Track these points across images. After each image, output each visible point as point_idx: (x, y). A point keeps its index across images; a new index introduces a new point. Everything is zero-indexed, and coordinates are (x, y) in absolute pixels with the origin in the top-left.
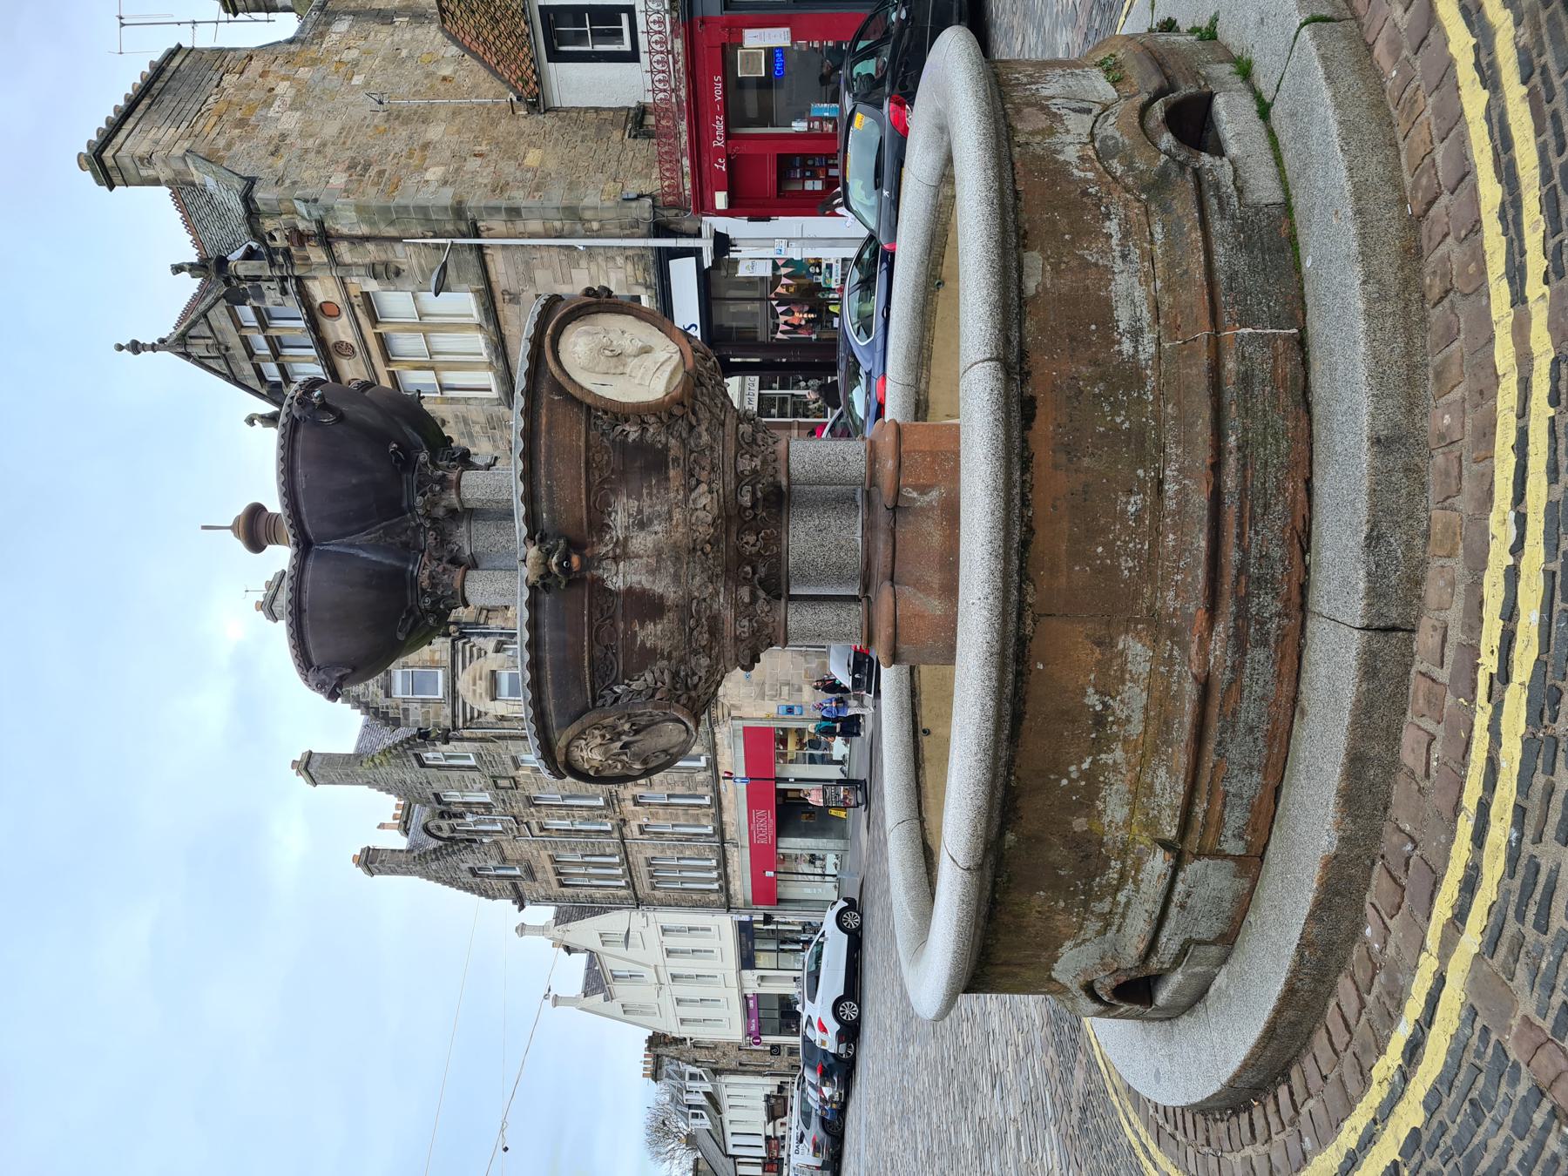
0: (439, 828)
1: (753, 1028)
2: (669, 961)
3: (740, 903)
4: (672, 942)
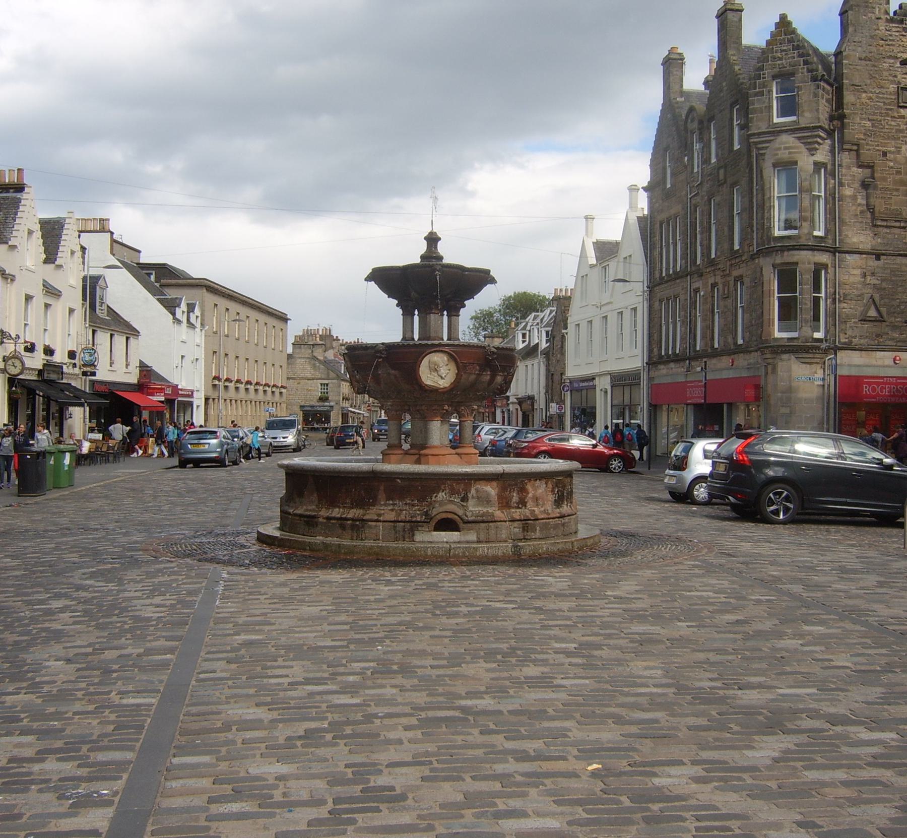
0: (692, 121)
1: (576, 385)
2: (615, 313)
3: (652, 374)
4: (627, 315)
